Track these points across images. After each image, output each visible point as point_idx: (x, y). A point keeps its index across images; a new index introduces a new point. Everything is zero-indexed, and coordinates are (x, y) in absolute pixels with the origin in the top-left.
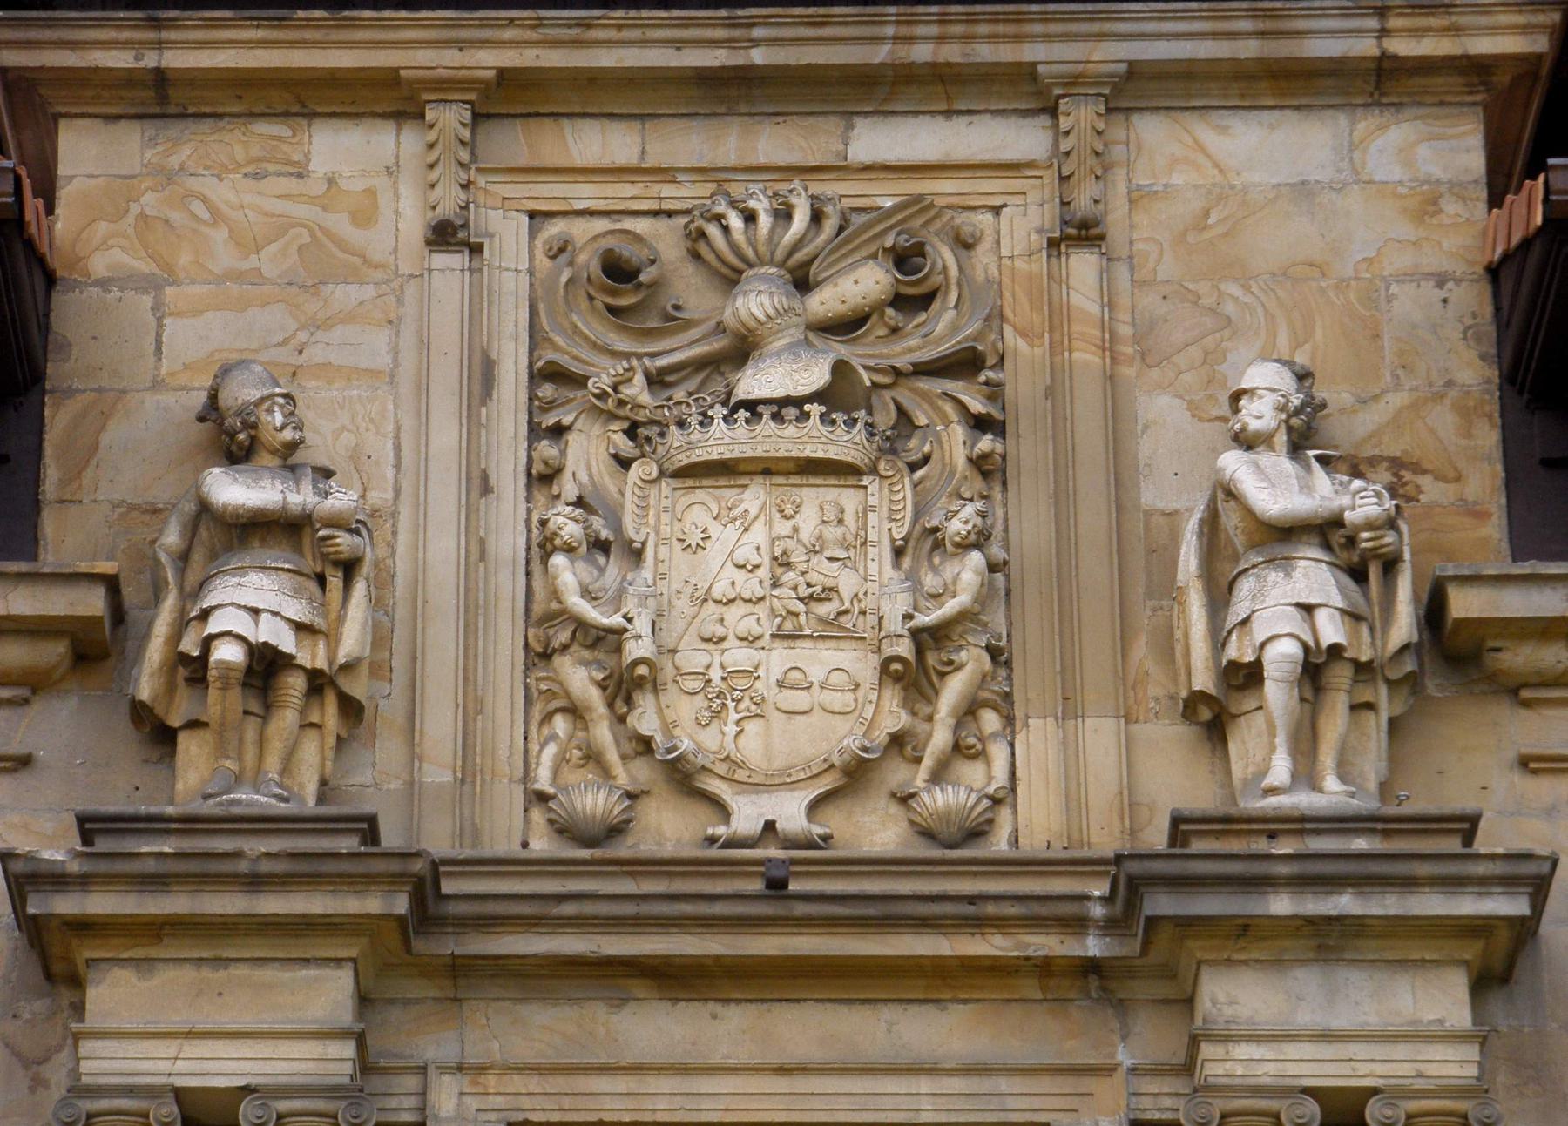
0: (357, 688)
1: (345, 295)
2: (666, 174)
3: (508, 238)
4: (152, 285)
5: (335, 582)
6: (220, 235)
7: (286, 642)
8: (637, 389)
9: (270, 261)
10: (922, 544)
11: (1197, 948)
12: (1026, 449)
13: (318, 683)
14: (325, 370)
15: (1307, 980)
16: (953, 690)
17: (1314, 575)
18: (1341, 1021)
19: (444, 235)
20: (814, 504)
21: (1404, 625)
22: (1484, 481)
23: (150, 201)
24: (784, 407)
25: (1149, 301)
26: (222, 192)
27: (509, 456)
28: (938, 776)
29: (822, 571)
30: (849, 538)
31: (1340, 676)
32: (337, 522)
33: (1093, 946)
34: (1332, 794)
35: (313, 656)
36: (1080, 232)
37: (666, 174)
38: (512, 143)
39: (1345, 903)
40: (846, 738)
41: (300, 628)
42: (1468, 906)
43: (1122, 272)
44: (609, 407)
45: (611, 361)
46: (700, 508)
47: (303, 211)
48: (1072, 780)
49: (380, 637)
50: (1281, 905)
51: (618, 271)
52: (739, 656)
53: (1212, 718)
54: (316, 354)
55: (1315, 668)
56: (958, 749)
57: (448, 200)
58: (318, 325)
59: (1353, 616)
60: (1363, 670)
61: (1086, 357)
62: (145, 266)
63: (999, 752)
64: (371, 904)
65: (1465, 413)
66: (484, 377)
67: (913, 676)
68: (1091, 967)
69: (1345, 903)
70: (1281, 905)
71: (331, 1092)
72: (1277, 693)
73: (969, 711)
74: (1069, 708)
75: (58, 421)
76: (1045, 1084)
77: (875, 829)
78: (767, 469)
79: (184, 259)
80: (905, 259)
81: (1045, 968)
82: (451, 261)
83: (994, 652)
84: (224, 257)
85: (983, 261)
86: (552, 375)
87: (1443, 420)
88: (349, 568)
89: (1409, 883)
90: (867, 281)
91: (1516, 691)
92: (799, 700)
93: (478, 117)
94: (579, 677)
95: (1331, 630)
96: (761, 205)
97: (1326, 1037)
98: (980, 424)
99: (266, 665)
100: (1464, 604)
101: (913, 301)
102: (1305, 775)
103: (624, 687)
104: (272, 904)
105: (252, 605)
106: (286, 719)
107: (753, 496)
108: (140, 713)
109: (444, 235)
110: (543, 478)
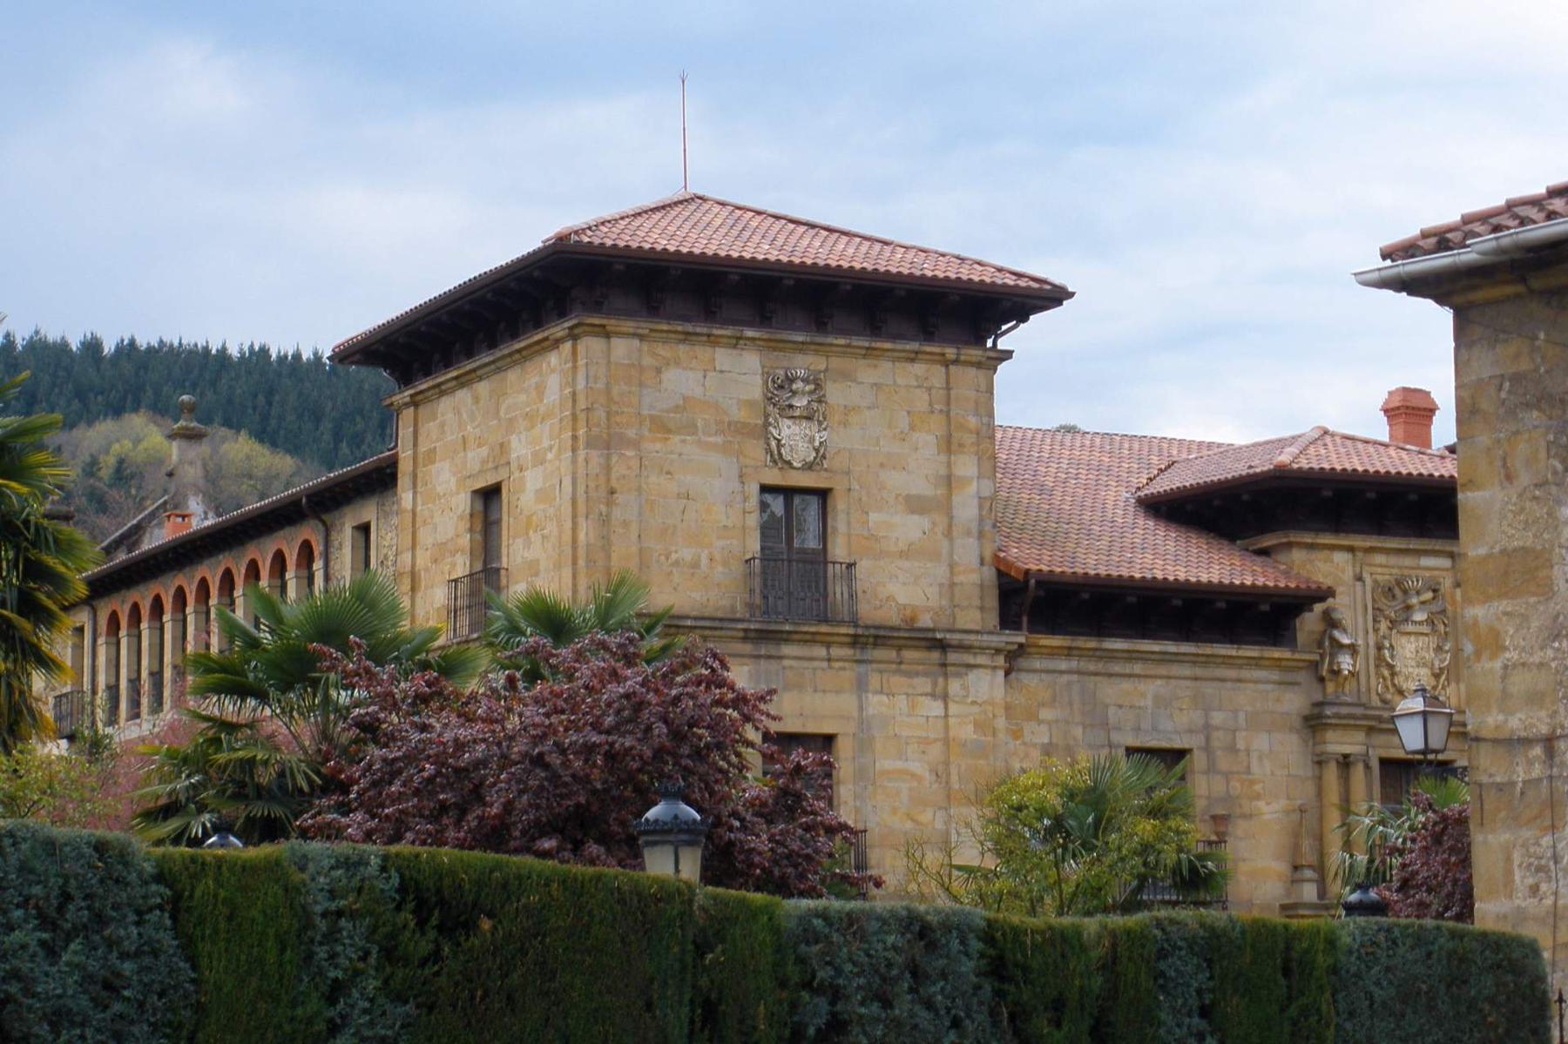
10: (1439, 649)
24: (1421, 623)
26: (1320, 564)
36: (1458, 585)
46: (1404, 640)
74: (1458, 682)
80: (1435, 591)
82: (1358, 584)
90: (1429, 595)
107: (1412, 638)
110: (1376, 630)
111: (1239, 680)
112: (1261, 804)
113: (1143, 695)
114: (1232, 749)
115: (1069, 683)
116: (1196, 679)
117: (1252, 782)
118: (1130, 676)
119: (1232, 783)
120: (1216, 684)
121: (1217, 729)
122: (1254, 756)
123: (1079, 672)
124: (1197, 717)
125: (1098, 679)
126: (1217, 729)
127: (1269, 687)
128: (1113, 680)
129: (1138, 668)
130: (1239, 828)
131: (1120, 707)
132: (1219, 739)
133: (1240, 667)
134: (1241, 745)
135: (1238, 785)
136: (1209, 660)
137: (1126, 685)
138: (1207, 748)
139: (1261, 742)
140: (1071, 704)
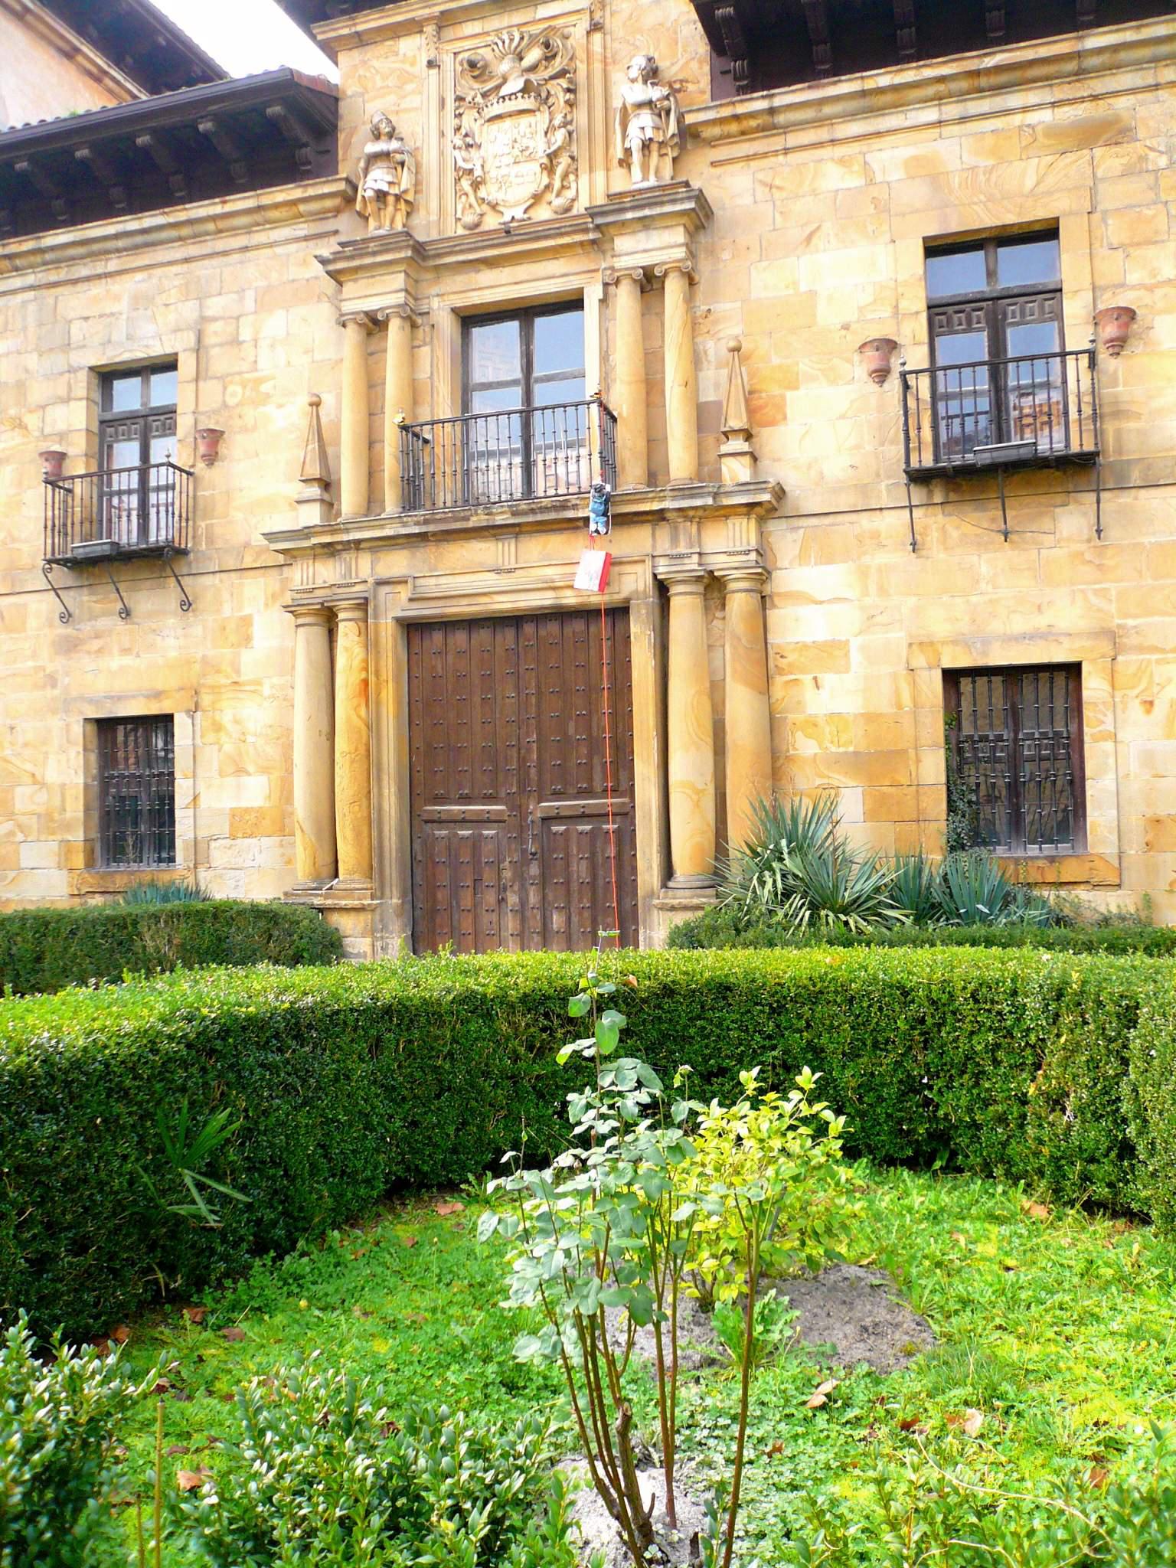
0: (410, 197)
1: (409, 87)
2: (487, 33)
3: (447, 60)
4: (362, 95)
5: (399, 168)
6: (378, 78)
7: (385, 188)
8: (479, 99)
9: (390, 82)
11: (612, 231)
12: (582, 95)
13: (398, 197)
14: (406, 110)
15: (642, 236)
16: (559, 170)
17: (646, 118)
18: (650, 246)
19: (431, 64)
20: (525, 120)
21: (673, 128)
22: (705, 82)
23: (361, 72)
25: (616, 45)
26: (376, 63)
27: (451, 123)
28: (558, 195)
29: (525, 142)
30: (533, 133)
31: (654, 147)
32: (395, 152)
33: (591, 236)
34: (652, 182)
35: (395, 190)
36: (596, 27)
37: (487, 33)
38: (449, 33)
39: (647, 212)
40: (532, 189)
41: (390, 183)
42: (678, 207)
43: (608, 37)
44: (473, 105)
45: (472, 89)
47: (397, 65)
48: (589, 190)
49: (417, 184)
50: (629, 215)
51: (472, 65)
52: (504, 171)
53: (625, 162)
54: (403, 106)
55: (646, 146)
56: (563, 187)
57: (432, 54)
58: (404, 97)
59: (657, 128)
60: (661, 144)
61: (598, 66)
62: (360, 90)
63: (573, 185)
64: (402, 255)
65: (700, 62)
66: (442, 103)
67: (550, 169)
68: (593, 242)
69: (647, 212)
70: (629, 215)
71: (399, 306)
72: (636, 157)
73: (565, 176)
75: (342, 137)
76: (583, 276)
77: (543, 213)
78: (510, 115)
79: (370, 85)
80: (547, 45)
81: (581, 244)
82: (434, 71)
83: (572, 158)
84: (379, 83)
85: (570, 42)
86: (460, 99)
87: (694, 65)
88: (402, 164)
89: (662, 203)
91: (711, 143)
92: (521, 180)
93: (440, 28)
94: (465, 184)
95: (649, 133)
96: (506, 37)
97: (645, 251)
98: (569, 90)
99: (381, 196)
100: (690, 119)
101: (549, 58)
102: (645, 178)
103: (476, 185)
104: (379, 259)
105: (378, 178)
106: (390, 208)
108: (359, 213)
109: (431, 64)
111: (246, 249)
112: (270, 409)
113: (117, 298)
114: (236, 342)
115: (24, 303)
116: (186, 260)
117: (260, 381)
118: (99, 277)
119: (231, 389)
120: (215, 262)
121: (215, 319)
122: (263, 344)
123: (32, 288)
124: (189, 311)
125: (59, 290)
126: (215, 319)
127: (293, 247)
128: (80, 287)
129: (113, 265)
130: (235, 447)
131: (86, 319)
132: (215, 333)
133: (248, 229)
134: (246, 334)
135: (239, 389)
136: (195, 231)
137: (97, 289)
138: (199, 348)
139: (275, 323)
140: (25, 329)
